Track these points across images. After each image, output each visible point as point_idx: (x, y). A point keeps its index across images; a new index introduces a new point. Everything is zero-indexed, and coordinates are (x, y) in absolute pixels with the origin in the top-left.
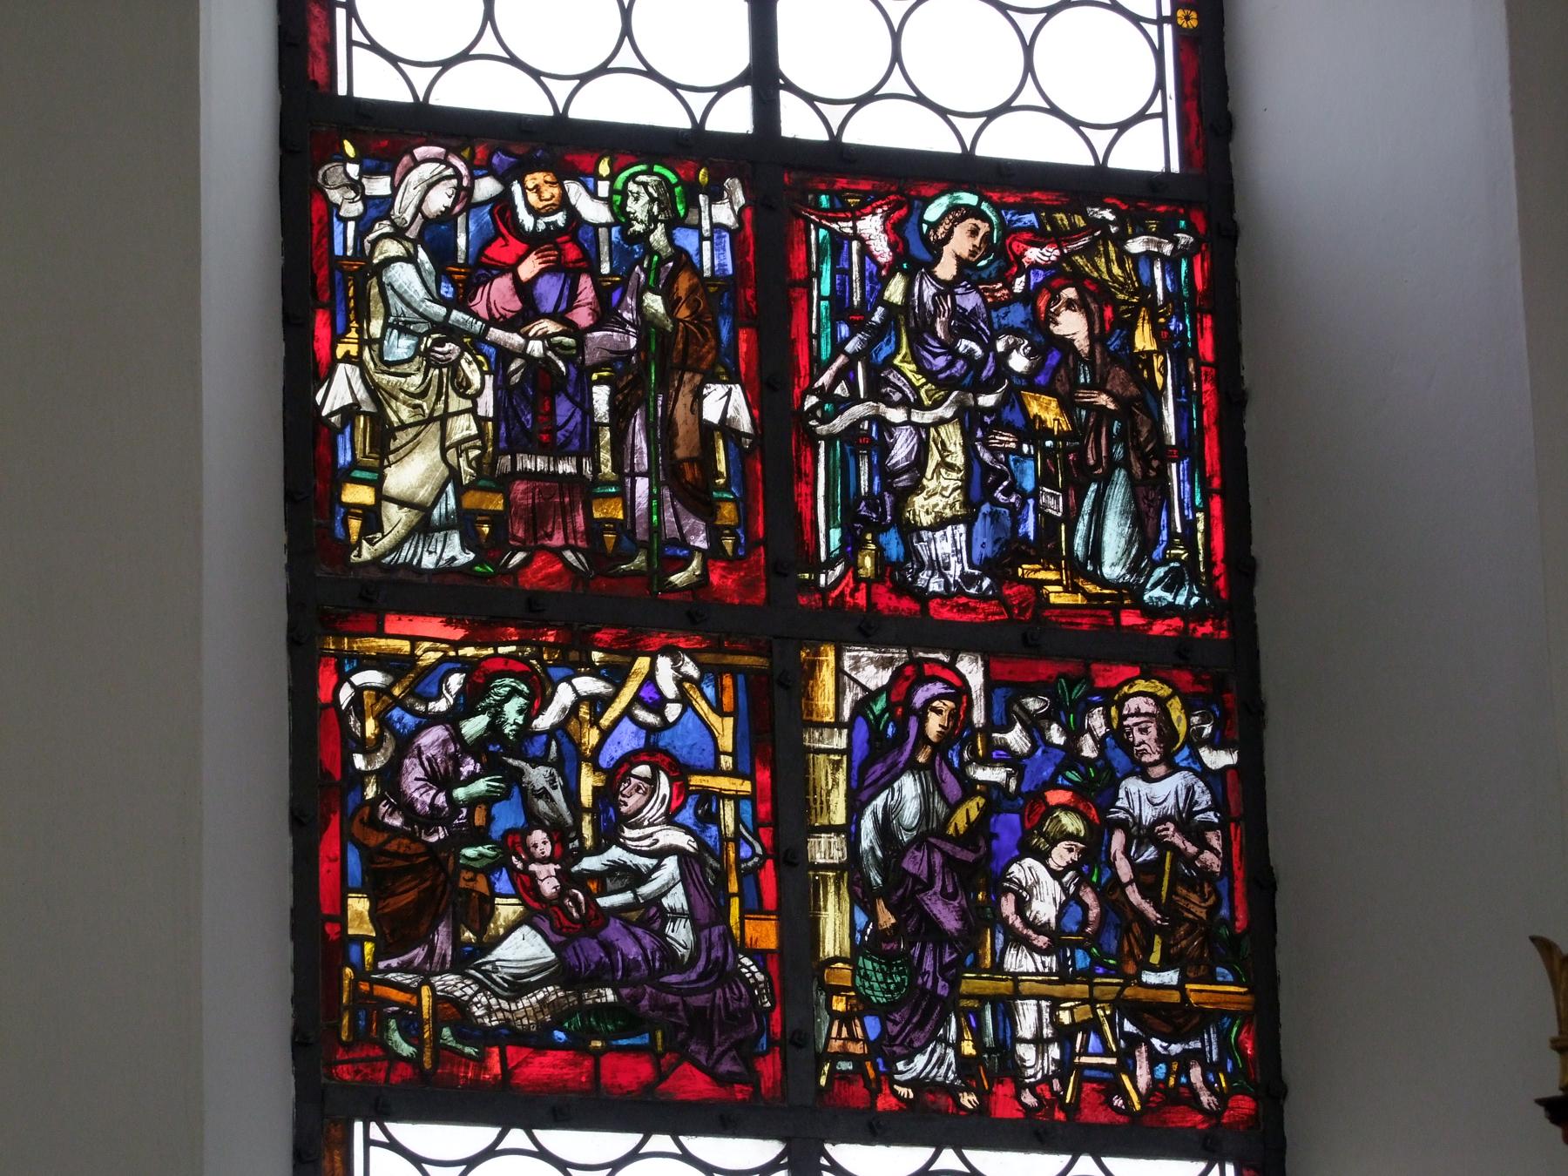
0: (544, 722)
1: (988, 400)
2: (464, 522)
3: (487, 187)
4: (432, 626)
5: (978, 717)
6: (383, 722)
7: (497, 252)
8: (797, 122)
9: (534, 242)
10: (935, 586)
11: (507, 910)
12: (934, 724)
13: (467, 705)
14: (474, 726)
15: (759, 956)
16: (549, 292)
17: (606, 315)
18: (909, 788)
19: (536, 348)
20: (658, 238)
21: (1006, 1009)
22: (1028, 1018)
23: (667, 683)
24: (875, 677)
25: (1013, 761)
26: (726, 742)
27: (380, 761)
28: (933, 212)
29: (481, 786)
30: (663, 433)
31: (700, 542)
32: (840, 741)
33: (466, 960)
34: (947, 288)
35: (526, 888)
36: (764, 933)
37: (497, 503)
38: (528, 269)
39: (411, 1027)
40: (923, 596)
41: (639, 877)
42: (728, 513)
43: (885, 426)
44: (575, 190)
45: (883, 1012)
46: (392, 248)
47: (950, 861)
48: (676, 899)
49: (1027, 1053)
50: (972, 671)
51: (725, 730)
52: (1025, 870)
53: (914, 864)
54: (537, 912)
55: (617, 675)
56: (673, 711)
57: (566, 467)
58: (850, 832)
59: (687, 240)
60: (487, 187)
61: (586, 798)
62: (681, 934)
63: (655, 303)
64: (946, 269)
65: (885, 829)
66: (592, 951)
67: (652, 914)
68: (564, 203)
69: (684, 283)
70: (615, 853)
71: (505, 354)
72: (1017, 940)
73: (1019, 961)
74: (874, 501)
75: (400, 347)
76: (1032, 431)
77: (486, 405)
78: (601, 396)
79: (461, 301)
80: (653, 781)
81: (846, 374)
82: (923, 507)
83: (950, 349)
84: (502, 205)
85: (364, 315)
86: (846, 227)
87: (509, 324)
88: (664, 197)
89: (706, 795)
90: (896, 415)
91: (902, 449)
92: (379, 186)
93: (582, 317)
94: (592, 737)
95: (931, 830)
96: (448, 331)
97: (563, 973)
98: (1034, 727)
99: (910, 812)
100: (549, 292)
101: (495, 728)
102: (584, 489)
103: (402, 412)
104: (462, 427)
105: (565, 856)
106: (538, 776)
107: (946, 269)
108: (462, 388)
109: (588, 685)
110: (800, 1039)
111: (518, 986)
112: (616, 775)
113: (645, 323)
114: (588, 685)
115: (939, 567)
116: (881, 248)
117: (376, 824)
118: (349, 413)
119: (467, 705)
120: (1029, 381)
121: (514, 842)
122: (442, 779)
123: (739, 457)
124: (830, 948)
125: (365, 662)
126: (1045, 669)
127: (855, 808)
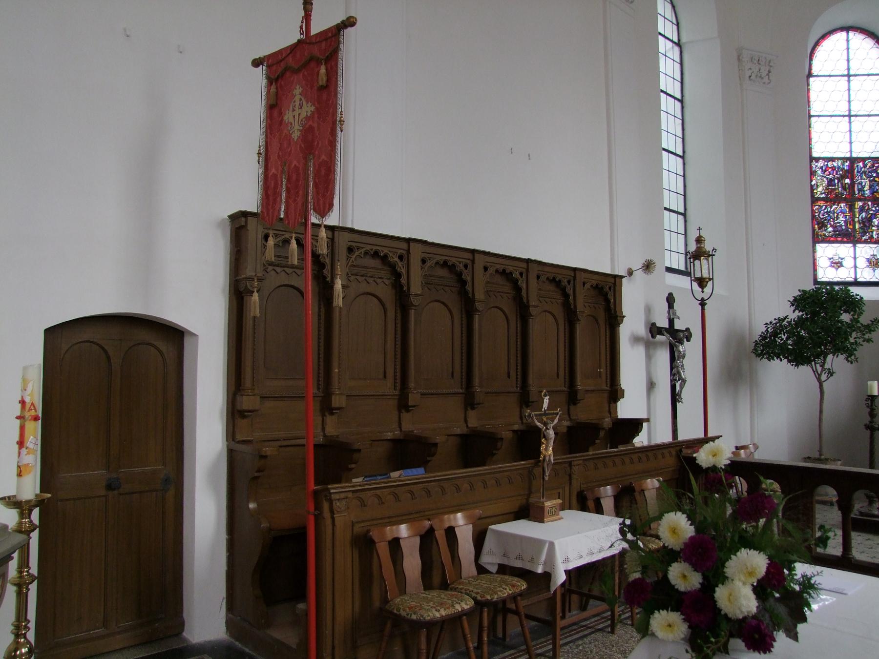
0: (832, 210)
1: (872, 179)
2: (824, 193)
3: (826, 163)
4: (822, 202)
5: (870, 207)
6: (818, 211)
7: (827, 169)
8: (854, 155)
9: (830, 168)
10: (866, 196)
11: (829, 226)
12: (866, 208)
13: (825, 209)
14: (826, 211)
15: (851, 229)
16: (832, 172)
17: (837, 174)
18: (864, 214)
19: (830, 177)
20: (841, 167)
21: (872, 232)
22: (875, 233)
23: (842, 206)
24: (861, 204)
25: (874, 211)
26: (848, 211)
27: (818, 214)
28: (867, 162)
29: (827, 216)
30: (842, 184)
31: (845, 193)
32: (858, 210)
33: (825, 230)
34: (868, 169)
35: (830, 224)
36: (851, 227)
37: (827, 191)
38: (830, 170)
39: (821, 236)
40: (865, 197)
41: (840, 223)
42: (848, 191)
43: (862, 182)
44: (834, 163)
45: (862, 233)
46: (818, 169)
47: (868, 220)
48: (843, 224)
49: (874, 236)
50: (870, 203)
51: (847, 210)
52: (874, 220)
53: (864, 220)
54: (832, 226)
55: (838, 205)
56: (843, 208)
57: (833, 188)
58: (859, 218)
59: (844, 167)
60: (826, 163)
61: (835, 216)
62: (844, 227)
63: (841, 172)
64: (868, 167)
65: (862, 218)
66: (836, 229)
67: (841, 226)
68: (833, 164)
69: (844, 171)
70: (838, 221)
71: (828, 178)
72: (874, 226)
73: (873, 228)
74: (861, 189)
75: (819, 178)
76: (876, 181)
77: (826, 183)
78: (836, 181)
79: (824, 174)
80: (841, 215)
81: (858, 177)
82: (865, 189)
83: (868, 174)
84: (827, 165)
85: (815, 175)
86: (858, 164)
87: (829, 175)
88: (842, 163)
89: (846, 216)
90: (863, 181)
91: (863, 184)
92: (816, 164)
93: (834, 174)
94: (836, 211)
95: (866, 217)
96: (823, 176)
97: (834, 231)
98: (875, 207)
99: (864, 216)
100: (832, 172)
101: (827, 211)
102: (835, 189)
103: (819, 184)
104: (824, 185)
105: (834, 221)
106: (831, 214)
107: (868, 167)
108: (824, 181)
109: (836, 206)
110: (854, 236)
111: (830, 232)
112: (838, 214)
113: (840, 174)
114: (836, 206)
115: (867, 194)
116: (862, 166)
117: (817, 219)
118: (814, 184)
119: (825, 209)
120: (875, 177)
121: (829, 220)
122: (823, 215)
123: (849, 186)
124: (857, 228)
125: (816, 205)
126: (876, 202)
127: (859, 216)
